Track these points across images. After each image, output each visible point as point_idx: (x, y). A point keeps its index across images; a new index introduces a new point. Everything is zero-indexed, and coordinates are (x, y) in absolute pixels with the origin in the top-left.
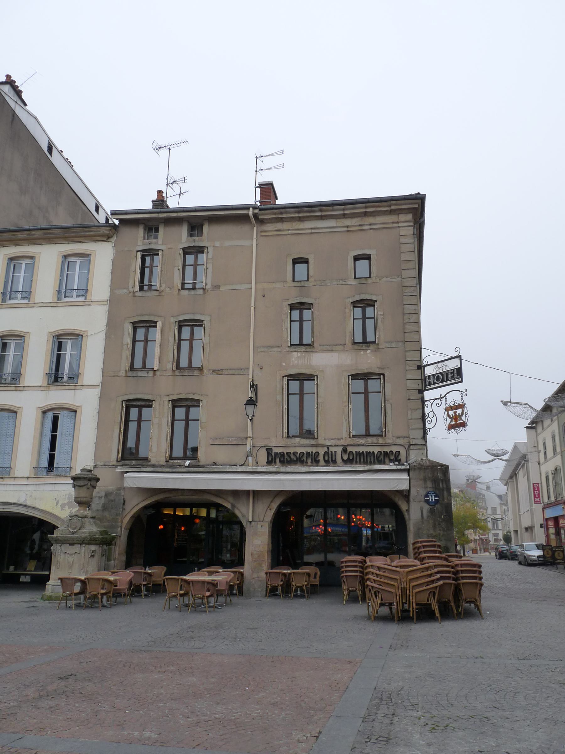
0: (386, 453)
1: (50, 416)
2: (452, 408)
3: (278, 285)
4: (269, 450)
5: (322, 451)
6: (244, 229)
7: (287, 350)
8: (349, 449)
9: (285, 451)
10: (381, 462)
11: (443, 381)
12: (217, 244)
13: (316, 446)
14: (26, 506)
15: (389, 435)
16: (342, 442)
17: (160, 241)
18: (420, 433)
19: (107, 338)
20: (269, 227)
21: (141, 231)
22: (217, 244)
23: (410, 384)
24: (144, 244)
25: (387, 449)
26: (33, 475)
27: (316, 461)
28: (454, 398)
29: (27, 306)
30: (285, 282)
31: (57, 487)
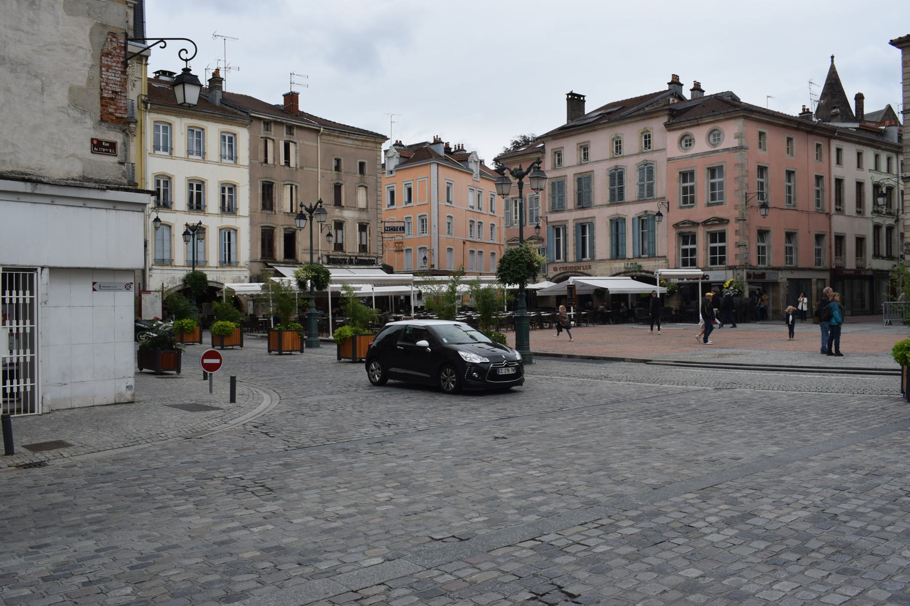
1: (223, 231)
2: (397, 243)
3: (329, 172)
4: (328, 256)
5: (348, 258)
6: (314, 135)
7: (333, 207)
8: (358, 258)
9: (335, 257)
10: (368, 264)
11: (394, 231)
12: (301, 142)
13: (346, 256)
14: (217, 283)
16: (355, 255)
17: (273, 134)
18: (380, 252)
19: (251, 189)
20: (324, 137)
21: (262, 125)
22: (301, 142)
23: (379, 230)
24: (264, 134)
26: (219, 266)
27: (345, 263)
28: (398, 238)
30: (331, 170)
31: (232, 273)
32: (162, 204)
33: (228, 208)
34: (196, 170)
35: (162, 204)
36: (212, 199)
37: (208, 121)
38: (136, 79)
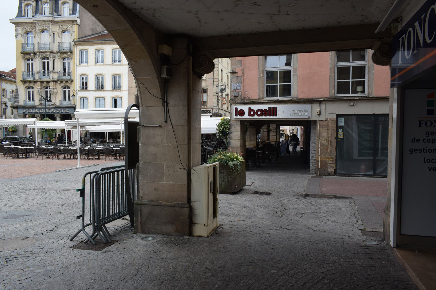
0: (207, 110)
1: (114, 99)
10: (206, 113)
15: (208, 105)
23: (214, 91)
25: (207, 109)
29: (103, 65)
32: (85, 88)
33: (116, 87)
34: (99, 70)
35: (85, 88)
36: (108, 84)
37: (105, 45)
38: (73, 32)
